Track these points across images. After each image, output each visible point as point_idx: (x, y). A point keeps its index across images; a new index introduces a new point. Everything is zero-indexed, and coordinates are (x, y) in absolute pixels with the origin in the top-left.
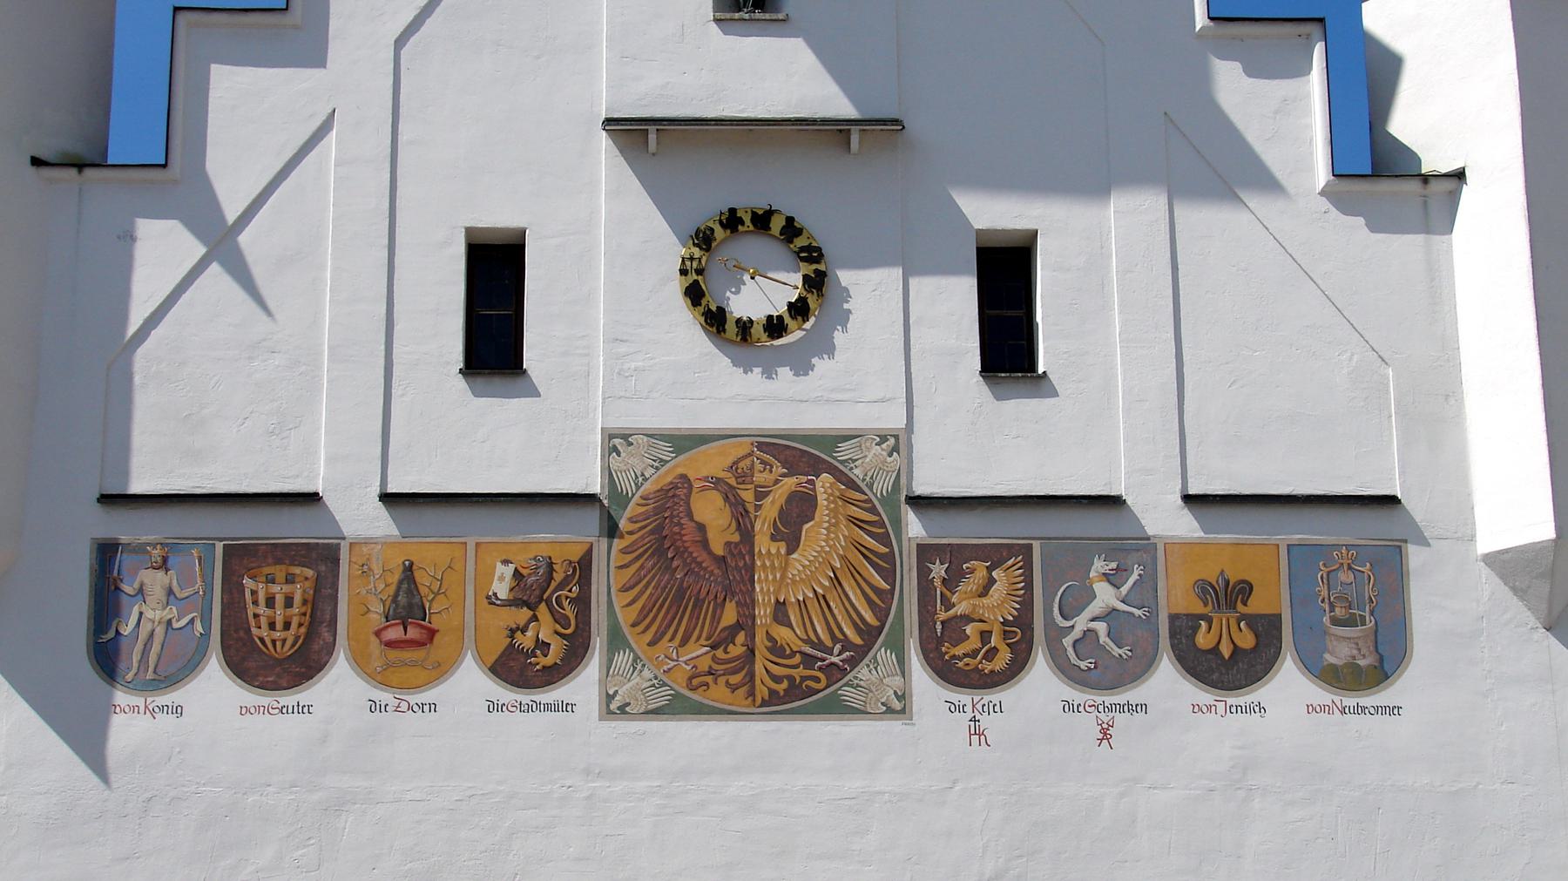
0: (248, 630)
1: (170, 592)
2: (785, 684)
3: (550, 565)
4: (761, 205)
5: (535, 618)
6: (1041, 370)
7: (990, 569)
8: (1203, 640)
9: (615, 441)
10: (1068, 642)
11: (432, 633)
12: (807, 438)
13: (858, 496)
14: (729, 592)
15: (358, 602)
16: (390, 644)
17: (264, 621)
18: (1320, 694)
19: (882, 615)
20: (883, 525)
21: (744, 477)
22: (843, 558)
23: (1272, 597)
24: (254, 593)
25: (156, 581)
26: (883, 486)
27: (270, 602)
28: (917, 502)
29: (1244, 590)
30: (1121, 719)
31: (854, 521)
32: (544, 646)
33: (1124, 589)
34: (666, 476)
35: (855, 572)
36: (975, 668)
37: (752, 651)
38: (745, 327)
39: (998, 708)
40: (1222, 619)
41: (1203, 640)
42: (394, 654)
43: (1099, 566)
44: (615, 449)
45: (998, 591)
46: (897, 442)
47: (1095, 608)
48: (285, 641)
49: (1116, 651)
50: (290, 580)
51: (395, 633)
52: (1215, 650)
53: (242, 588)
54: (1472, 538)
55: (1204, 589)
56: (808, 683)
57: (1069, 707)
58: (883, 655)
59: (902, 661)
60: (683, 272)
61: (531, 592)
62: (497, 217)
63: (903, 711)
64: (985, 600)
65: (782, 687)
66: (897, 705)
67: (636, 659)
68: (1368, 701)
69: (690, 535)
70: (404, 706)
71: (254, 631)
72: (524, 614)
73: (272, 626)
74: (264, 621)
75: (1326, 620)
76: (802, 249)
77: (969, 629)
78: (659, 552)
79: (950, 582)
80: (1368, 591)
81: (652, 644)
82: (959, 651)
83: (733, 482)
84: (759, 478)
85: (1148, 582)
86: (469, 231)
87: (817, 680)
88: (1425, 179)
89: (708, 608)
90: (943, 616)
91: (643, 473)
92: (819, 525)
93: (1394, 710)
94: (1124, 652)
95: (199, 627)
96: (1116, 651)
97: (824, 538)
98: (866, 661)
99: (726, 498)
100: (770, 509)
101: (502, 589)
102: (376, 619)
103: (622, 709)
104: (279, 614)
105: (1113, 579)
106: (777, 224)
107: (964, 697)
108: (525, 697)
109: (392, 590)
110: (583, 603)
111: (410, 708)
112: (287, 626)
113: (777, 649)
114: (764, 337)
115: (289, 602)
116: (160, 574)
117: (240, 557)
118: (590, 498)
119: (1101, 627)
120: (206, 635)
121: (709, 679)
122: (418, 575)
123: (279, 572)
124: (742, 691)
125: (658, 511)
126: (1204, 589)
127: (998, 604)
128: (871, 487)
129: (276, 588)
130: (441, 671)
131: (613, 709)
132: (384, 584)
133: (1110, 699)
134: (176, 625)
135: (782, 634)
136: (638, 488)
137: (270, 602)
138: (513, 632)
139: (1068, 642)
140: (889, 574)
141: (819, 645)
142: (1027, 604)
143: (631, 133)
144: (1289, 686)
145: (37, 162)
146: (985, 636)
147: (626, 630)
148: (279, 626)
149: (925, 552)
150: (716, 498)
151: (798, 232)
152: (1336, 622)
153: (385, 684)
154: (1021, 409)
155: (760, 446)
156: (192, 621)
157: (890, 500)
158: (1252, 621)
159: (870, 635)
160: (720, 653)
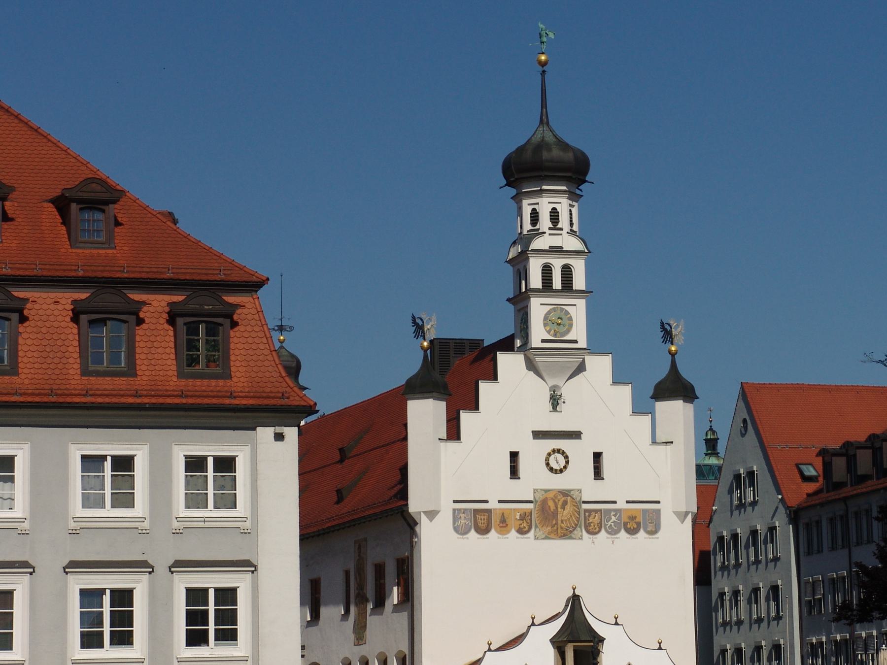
8: (629, 526)
9: (535, 491)
15: (495, 519)
18: (646, 535)
21: (556, 497)
23: (640, 519)
25: (463, 516)
26: (578, 499)
29: (635, 517)
34: (544, 497)
38: (556, 470)
40: (632, 523)
41: (629, 526)
43: (613, 513)
46: (580, 491)
48: (483, 526)
56: (566, 534)
58: (578, 529)
61: (522, 518)
79: (589, 516)
85: (620, 516)
91: (540, 497)
97: (569, 508)
100: (560, 503)
105: (615, 515)
113: (562, 528)
117: (476, 511)
127: (597, 520)
130: (508, 532)
131: (536, 538)
144: (642, 533)
149: (585, 511)
159: (576, 525)
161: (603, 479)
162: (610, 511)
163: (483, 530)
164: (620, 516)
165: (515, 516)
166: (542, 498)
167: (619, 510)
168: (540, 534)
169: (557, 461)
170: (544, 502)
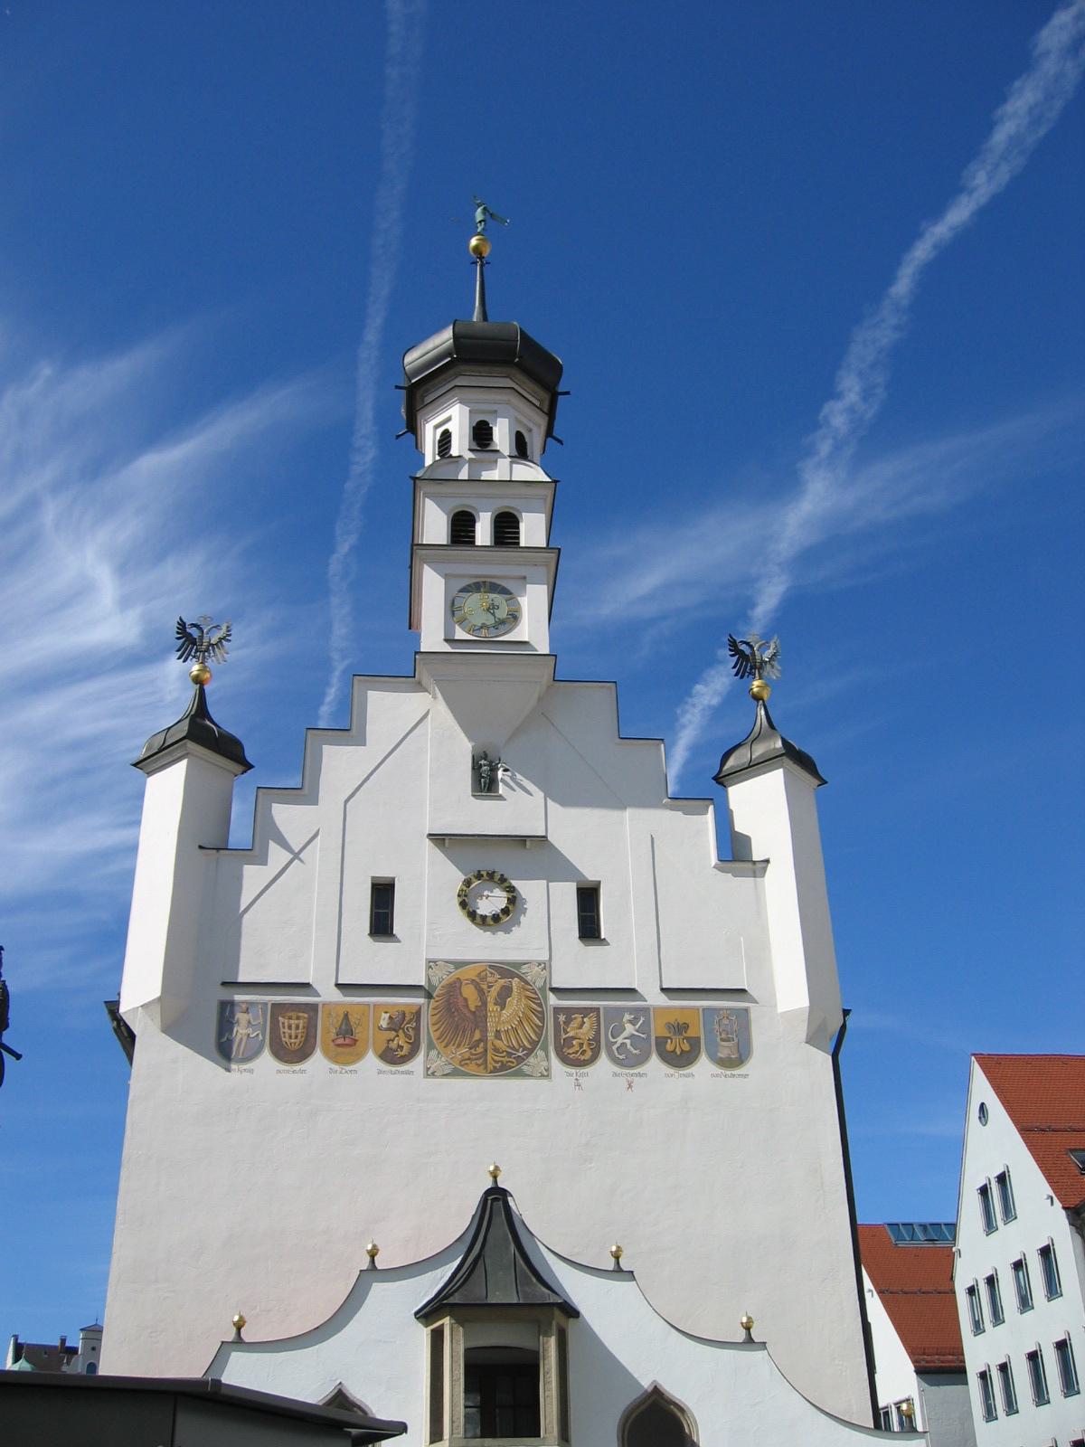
0: (280, 1039)
1: (249, 1022)
2: (500, 1064)
3: (404, 1014)
4: (491, 869)
5: (398, 1036)
6: (603, 937)
7: (583, 1018)
8: (669, 1047)
9: (431, 964)
10: (614, 1048)
11: (356, 1041)
12: (508, 964)
13: (530, 987)
14: (477, 1027)
15: (325, 1028)
16: (338, 1045)
17: (287, 1035)
19: (539, 1036)
20: (539, 999)
21: (484, 979)
22: (523, 1013)
24: (283, 1023)
26: (539, 983)
27: (290, 1027)
28: (553, 990)
29: (686, 1027)
30: (636, 1079)
31: (528, 997)
32: (401, 1047)
33: (637, 1026)
35: (528, 1019)
36: (578, 1059)
37: (486, 1050)
38: (484, 918)
39: (583, 1075)
40: (677, 1039)
41: (669, 1047)
42: (340, 1049)
43: (627, 1017)
44: (430, 967)
45: (586, 1026)
47: (625, 1034)
49: (634, 1052)
50: (298, 1018)
51: (341, 1041)
52: (674, 1051)
53: (278, 1022)
54: (776, 1006)
55: (669, 1026)
56: (509, 1064)
57: (615, 1074)
58: (540, 1053)
59: (547, 1056)
60: (459, 896)
61: (397, 1024)
62: (384, 872)
63: (548, 1076)
64: (581, 1031)
65: (498, 1065)
66: (546, 1074)
67: (439, 1053)
68: (736, 1072)
69: (461, 1003)
70: (344, 1071)
71: (283, 1039)
72: (394, 1033)
73: (290, 1037)
74: (287, 1035)
75: (718, 1039)
76: (508, 887)
77: (574, 1042)
78: (449, 1010)
79: (567, 1023)
80: (735, 1026)
81: (445, 1047)
82: (570, 1051)
83: (478, 981)
84: (489, 979)
85: (647, 1023)
86: (373, 878)
87: (513, 1063)
88: (754, 862)
89: (468, 1033)
90: (564, 1037)
91: (442, 977)
92: (513, 999)
93: (746, 1076)
94: (637, 1052)
95: (260, 1036)
96: (634, 1052)
97: (515, 1005)
98: (533, 1054)
99: (476, 987)
100: (494, 992)
101: (384, 1024)
102: (333, 1036)
103: (433, 1074)
104: (293, 1032)
105: (632, 1022)
106: (497, 877)
107: (572, 1070)
108: (394, 1068)
109: (340, 1023)
110: (417, 1029)
111: (346, 1072)
112: (296, 1037)
113: (496, 1050)
114: (492, 923)
115: (297, 1027)
116: (245, 1015)
117: (278, 1008)
118: (420, 987)
119: (628, 1041)
120: (264, 1040)
121: (468, 1062)
122: (350, 1017)
123: (294, 1014)
124: (482, 1067)
125: (448, 993)
126: (669, 1026)
127: (587, 1031)
128: (534, 983)
129: (292, 1022)
130: (359, 1057)
132: (337, 1021)
133: (632, 1072)
134: (251, 1036)
135: (498, 1043)
136: (440, 982)
137: (290, 1027)
138: (389, 1041)
139: (614, 1048)
140: (542, 1019)
141: (514, 1048)
142: (598, 1032)
143: (439, 839)
144: (704, 1066)
145: (201, 847)
146: (581, 1045)
147: (435, 1042)
148: (293, 1037)
149: (557, 1010)
150: (472, 987)
151: (505, 880)
152: (723, 1040)
153: (336, 1062)
154: (594, 950)
155: (490, 966)
156: (258, 1035)
157: (542, 989)
158: (688, 1039)
159: (534, 1044)
160: (473, 1051)
161: (603, 942)
162: (620, 1012)
163: (290, 1053)
164: (647, 1023)
165: (378, 1018)
166: (447, 980)
167: (645, 1010)
168: (438, 1063)
169: (491, 902)
170: (454, 988)
